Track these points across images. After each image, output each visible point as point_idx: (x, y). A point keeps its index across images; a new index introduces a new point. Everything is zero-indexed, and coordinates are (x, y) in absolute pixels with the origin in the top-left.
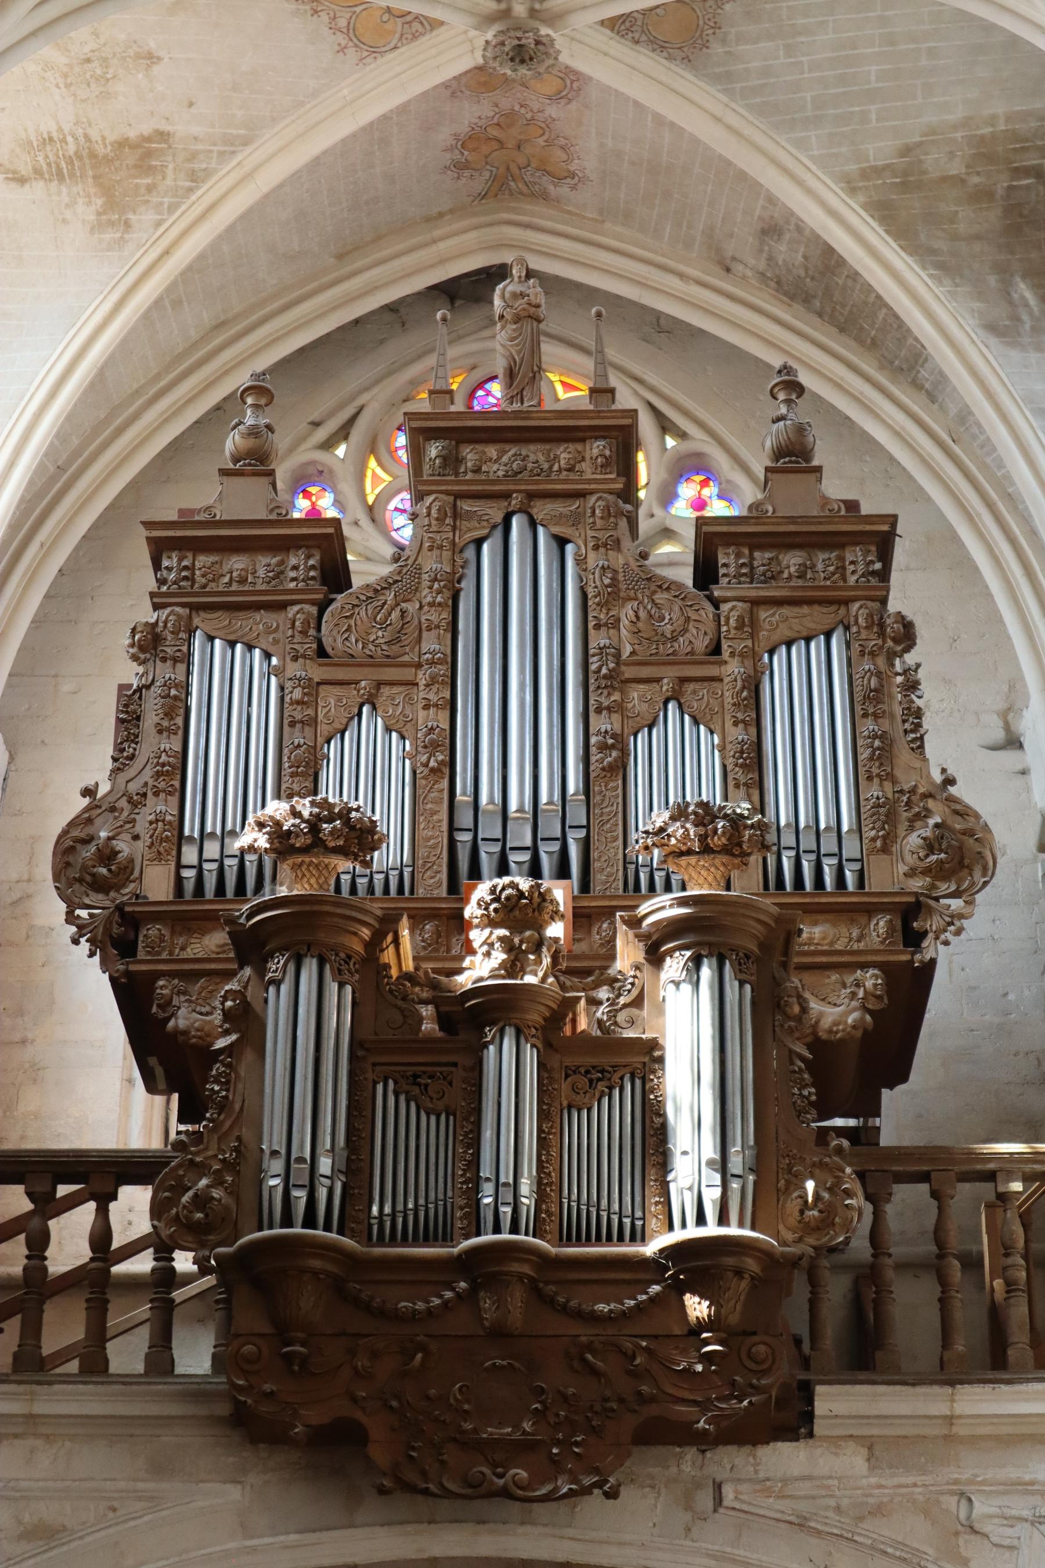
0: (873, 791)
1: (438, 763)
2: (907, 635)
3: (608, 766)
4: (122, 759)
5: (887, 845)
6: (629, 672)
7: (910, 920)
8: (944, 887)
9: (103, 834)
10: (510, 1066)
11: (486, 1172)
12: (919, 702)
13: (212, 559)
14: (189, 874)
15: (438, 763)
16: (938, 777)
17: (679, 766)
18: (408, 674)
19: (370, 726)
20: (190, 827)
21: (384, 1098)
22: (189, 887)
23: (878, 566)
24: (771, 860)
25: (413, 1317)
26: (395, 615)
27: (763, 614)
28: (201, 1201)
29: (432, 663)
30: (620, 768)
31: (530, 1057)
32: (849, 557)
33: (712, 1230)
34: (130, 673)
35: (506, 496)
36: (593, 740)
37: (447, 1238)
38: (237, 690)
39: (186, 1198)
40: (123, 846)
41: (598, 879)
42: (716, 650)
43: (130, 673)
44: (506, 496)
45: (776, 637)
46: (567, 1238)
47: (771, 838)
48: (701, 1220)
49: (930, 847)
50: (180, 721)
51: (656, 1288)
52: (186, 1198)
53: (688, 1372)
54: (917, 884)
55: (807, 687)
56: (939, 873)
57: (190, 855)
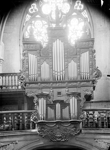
0: (91, 69)
1: (51, 67)
2: (95, 52)
3: (66, 67)
4: (23, 67)
5: (92, 74)
6: (68, 57)
7: (94, 82)
8: (97, 78)
9: (22, 75)
10: (58, 106)
11: (57, 115)
12: (95, 59)
13: (29, 45)
14: (30, 78)
15: (51, 67)
16: (97, 67)
17: (73, 65)
18: (48, 58)
19: (45, 63)
20: (30, 74)
21: (49, 108)
22: (30, 80)
23: (92, 44)
24: (81, 76)
25: (51, 127)
26: (47, 51)
27: (81, 50)
28: (35, 118)
29: (51, 57)
30: (67, 67)
31: (60, 105)
32: (90, 43)
33: (74, 120)
34: (22, 57)
35: (57, 37)
36: (65, 64)
37: (54, 120)
38: (32, 58)
39: (34, 118)
40: (24, 76)
41: (66, 79)
42: (76, 54)
43: (22, 57)
44: (57, 37)
45: (82, 52)
46: (63, 120)
47: (81, 73)
48: (73, 119)
49: (96, 75)
50: (28, 63)
51: (70, 124)
52: (34, 118)
53: (73, 131)
54: (94, 79)
55: (85, 57)
56: (96, 77)
57: (30, 77)
